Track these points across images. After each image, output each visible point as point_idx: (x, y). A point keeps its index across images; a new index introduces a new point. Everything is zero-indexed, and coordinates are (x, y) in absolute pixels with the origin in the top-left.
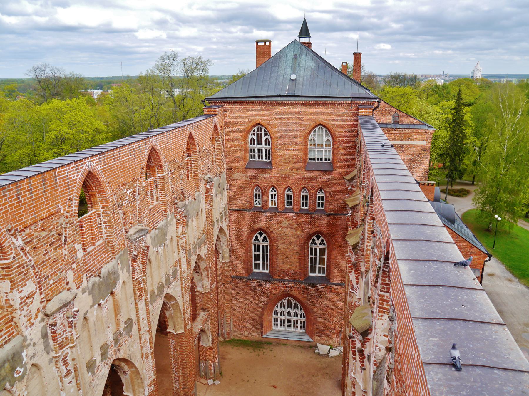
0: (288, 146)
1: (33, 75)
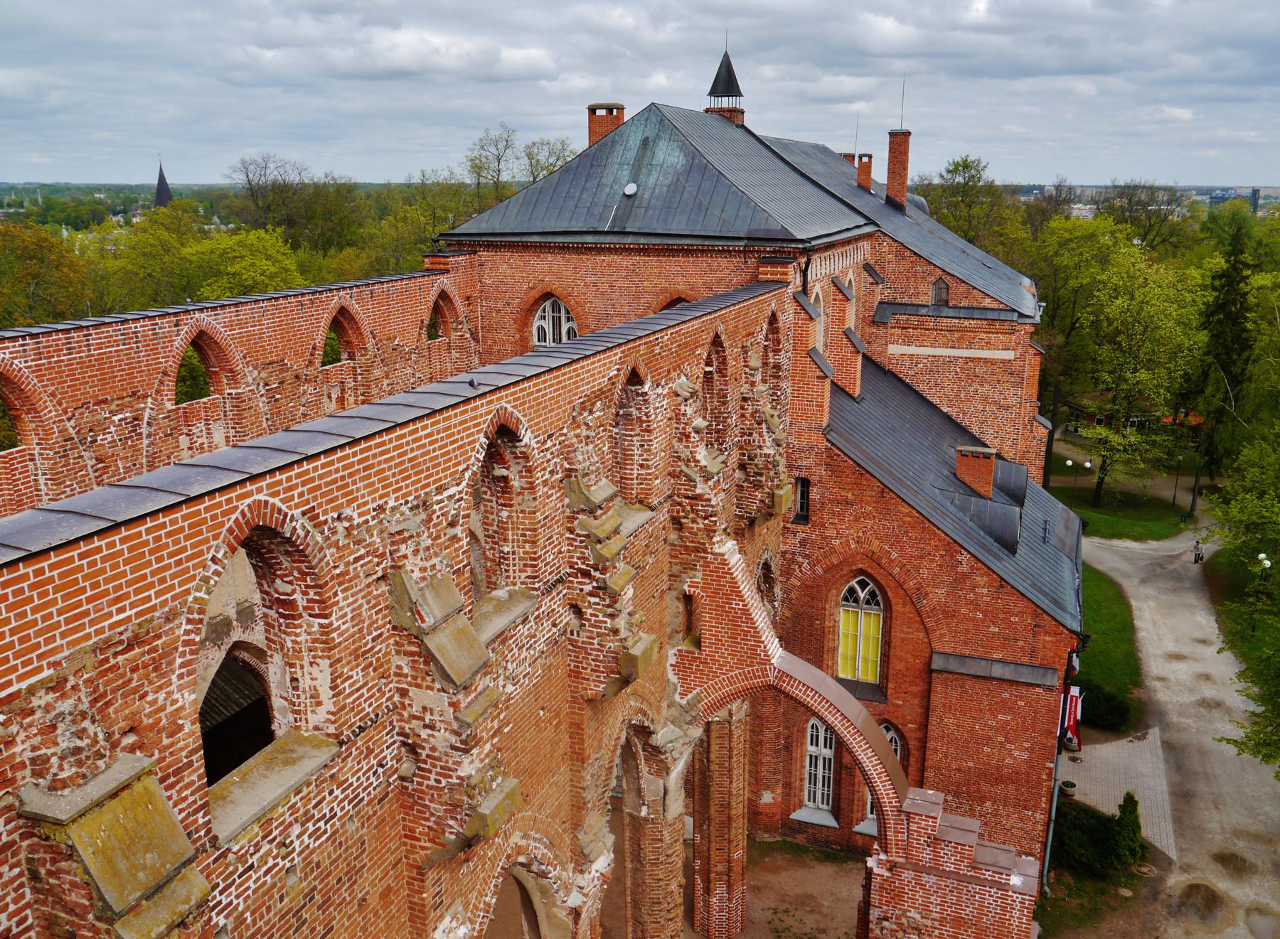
1: (240, 179)
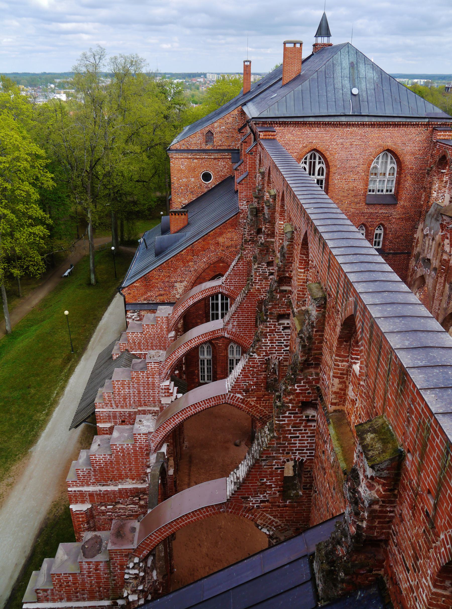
0: (349, 176)
